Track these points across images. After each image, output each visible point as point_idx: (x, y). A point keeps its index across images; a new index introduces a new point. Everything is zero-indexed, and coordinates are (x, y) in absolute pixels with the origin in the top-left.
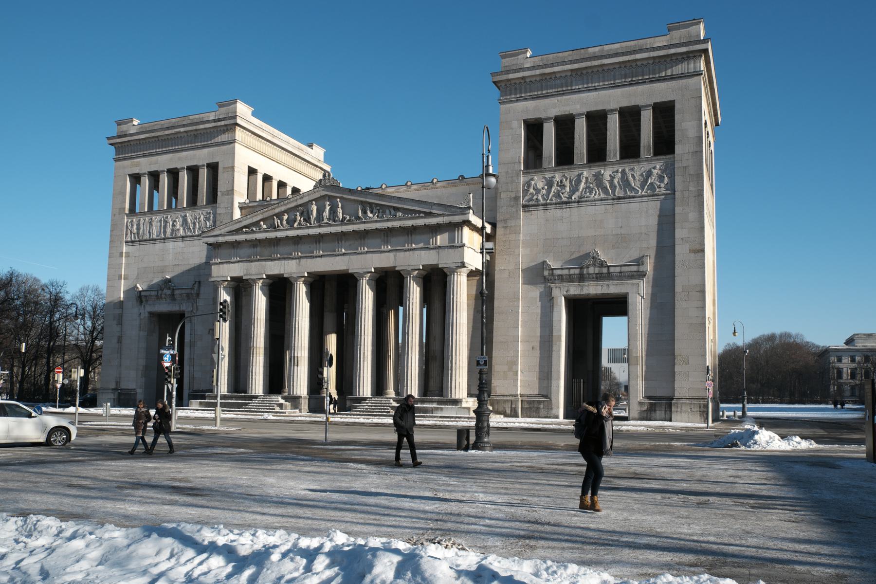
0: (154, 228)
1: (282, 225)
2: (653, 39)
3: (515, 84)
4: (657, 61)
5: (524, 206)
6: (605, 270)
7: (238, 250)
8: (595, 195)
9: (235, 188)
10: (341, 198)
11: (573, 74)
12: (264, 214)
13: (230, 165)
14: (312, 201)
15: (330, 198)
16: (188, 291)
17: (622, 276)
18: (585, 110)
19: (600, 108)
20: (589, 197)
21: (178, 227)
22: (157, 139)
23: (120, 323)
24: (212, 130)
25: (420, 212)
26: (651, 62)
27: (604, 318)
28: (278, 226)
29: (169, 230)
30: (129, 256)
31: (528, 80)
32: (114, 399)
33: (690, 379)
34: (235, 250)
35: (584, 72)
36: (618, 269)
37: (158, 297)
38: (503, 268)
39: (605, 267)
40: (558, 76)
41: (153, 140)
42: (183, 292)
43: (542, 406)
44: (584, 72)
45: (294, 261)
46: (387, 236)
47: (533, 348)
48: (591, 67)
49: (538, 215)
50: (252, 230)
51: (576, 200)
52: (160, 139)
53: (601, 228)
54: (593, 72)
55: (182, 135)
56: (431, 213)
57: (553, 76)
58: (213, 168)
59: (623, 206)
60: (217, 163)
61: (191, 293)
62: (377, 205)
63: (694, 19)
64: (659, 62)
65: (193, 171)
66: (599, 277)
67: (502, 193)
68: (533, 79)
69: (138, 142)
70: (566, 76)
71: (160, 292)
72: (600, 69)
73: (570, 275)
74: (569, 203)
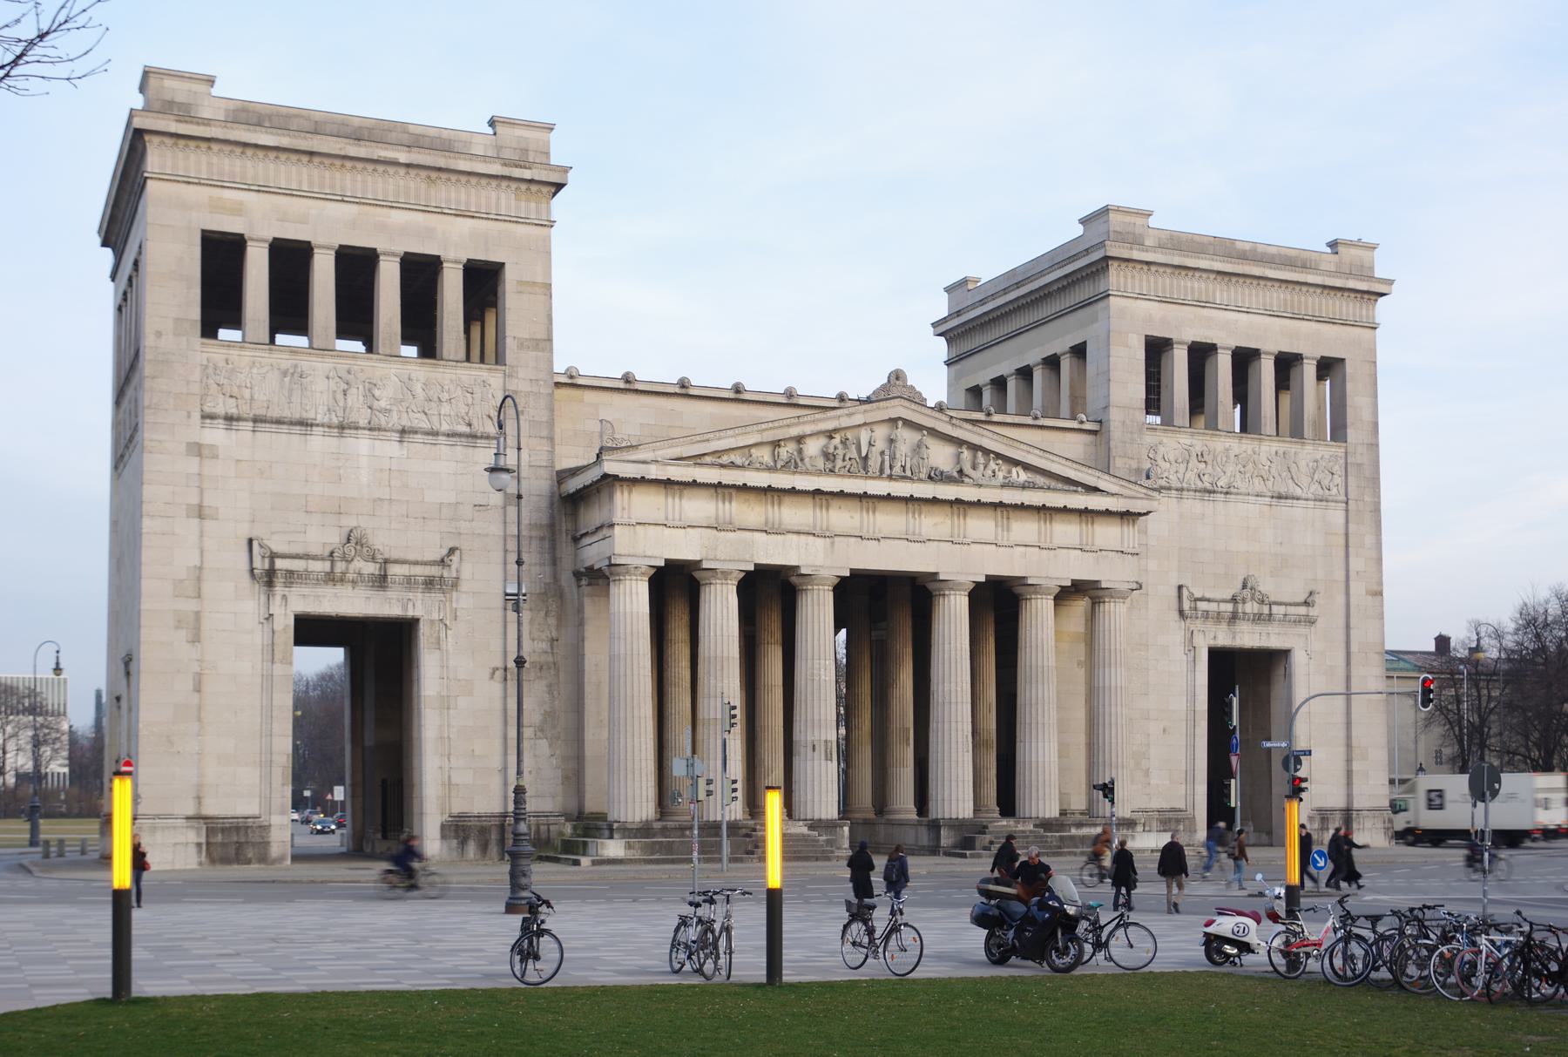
6: (1266, 610)
12: (765, 434)
13: (539, 279)
16: (434, 571)
18: (1234, 343)
19: (1253, 345)
21: (383, 404)
23: (196, 639)
32: (199, 845)
33: (1370, 782)
37: (331, 578)
42: (418, 570)
43: (1181, 827)
45: (820, 541)
47: (1164, 730)
51: (1225, 490)
56: (1096, 490)
59: (1284, 508)
61: (442, 577)
62: (999, 456)
66: (1258, 618)
67: (1117, 459)
71: (340, 567)
74: (1214, 492)
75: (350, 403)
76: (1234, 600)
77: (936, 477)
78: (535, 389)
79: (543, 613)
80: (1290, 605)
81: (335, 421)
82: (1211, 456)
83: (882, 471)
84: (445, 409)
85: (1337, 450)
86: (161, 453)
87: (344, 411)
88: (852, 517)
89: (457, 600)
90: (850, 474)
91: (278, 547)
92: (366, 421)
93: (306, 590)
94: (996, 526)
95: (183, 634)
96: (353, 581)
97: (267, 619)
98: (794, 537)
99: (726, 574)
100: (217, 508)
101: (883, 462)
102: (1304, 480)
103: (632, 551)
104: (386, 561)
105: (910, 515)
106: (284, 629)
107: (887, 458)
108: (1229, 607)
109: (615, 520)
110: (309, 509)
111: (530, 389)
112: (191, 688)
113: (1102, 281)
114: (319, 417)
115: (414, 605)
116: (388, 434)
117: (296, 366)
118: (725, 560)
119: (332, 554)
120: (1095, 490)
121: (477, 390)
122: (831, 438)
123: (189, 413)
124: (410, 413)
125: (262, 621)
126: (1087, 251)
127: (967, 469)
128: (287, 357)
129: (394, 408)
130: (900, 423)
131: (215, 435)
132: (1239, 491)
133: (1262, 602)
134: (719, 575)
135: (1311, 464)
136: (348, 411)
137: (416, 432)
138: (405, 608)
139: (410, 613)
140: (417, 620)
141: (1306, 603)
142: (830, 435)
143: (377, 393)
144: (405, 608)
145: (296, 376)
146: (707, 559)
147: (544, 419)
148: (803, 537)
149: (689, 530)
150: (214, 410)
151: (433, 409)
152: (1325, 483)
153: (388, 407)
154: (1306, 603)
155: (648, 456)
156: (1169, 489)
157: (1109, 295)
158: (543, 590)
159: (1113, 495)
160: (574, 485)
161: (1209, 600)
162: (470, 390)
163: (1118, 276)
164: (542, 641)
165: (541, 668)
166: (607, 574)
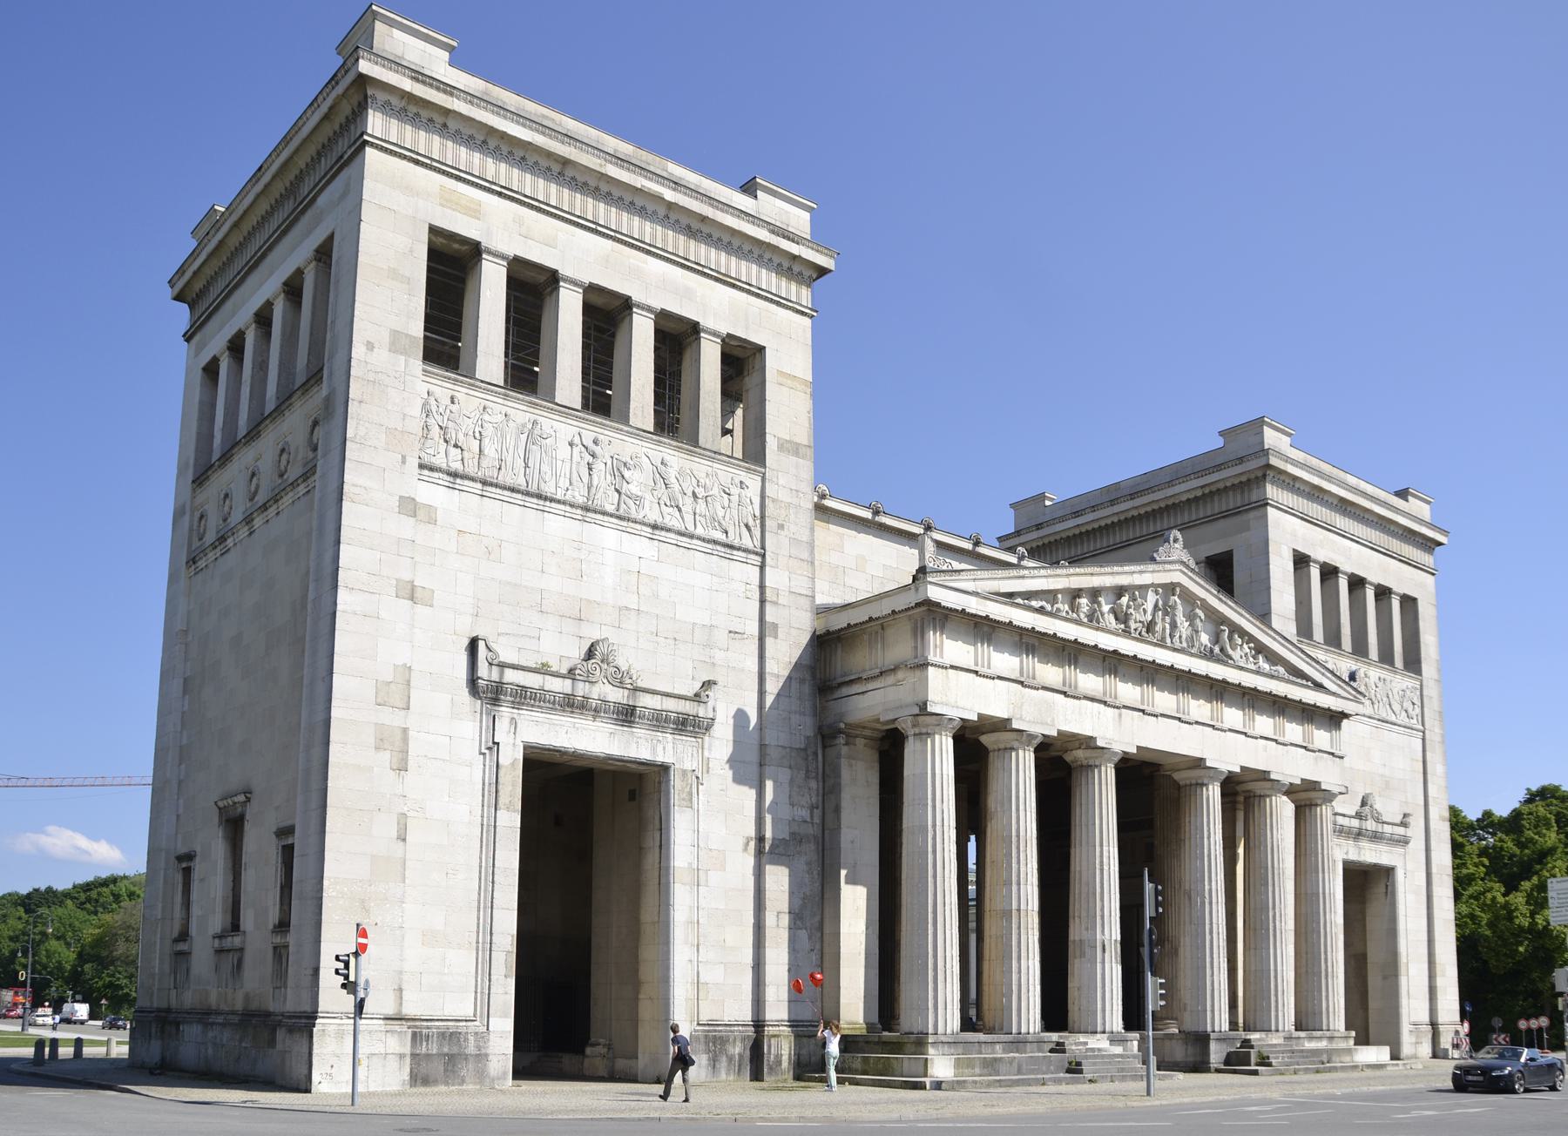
21: (634, 489)
23: (402, 767)
37: (570, 704)
42: (671, 705)
66: (1376, 837)
75: (595, 483)
77: (1208, 655)
78: (795, 501)
79: (802, 773)
81: (581, 500)
83: (1163, 639)
84: (701, 507)
85: (1401, 682)
87: (589, 489)
89: (710, 750)
90: (1140, 639)
91: (506, 656)
92: (613, 507)
93: (537, 715)
95: (385, 757)
96: (595, 710)
97: (490, 749)
98: (1089, 703)
99: (1031, 736)
100: (433, 591)
101: (1164, 629)
102: (1396, 707)
104: (636, 689)
106: (513, 764)
107: (1168, 626)
108: (1355, 823)
109: (931, 658)
110: (544, 608)
111: (789, 500)
112: (395, 834)
113: (1255, 491)
114: (559, 494)
115: (664, 748)
116: (638, 526)
117: (535, 423)
119: (571, 671)
120: (1319, 686)
121: (735, 491)
122: (1120, 596)
124: (663, 506)
125: (484, 751)
126: (1241, 460)
127: (1230, 652)
128: (525, 408)
129: (647, 497)
130: (1178, 590)
133: (1378, 820)
134: (1024, 738)
136: (593, 490)
137: (669, 530)
138: (654, 749)
139: (660, 758)
140: (664, 769)
142: (1119, 591)
143: (627, 474)
144: (654, 749)
145: (533, 436)
147: (805, 539)
148: (1096, 704)
150: (433, 460)
151: (687, 504)
152: (1410, 710)
153: (639, 494)
154: (1404, 824)
155: (969, 586)
157: (1267, 504)
158: (803, 746)
159: (1334, 694)
160: (839, 622)
161: (1344, 815)
162: (727, 490)
164: (803, 806)
165: (801, 842)
166: (905, 726)
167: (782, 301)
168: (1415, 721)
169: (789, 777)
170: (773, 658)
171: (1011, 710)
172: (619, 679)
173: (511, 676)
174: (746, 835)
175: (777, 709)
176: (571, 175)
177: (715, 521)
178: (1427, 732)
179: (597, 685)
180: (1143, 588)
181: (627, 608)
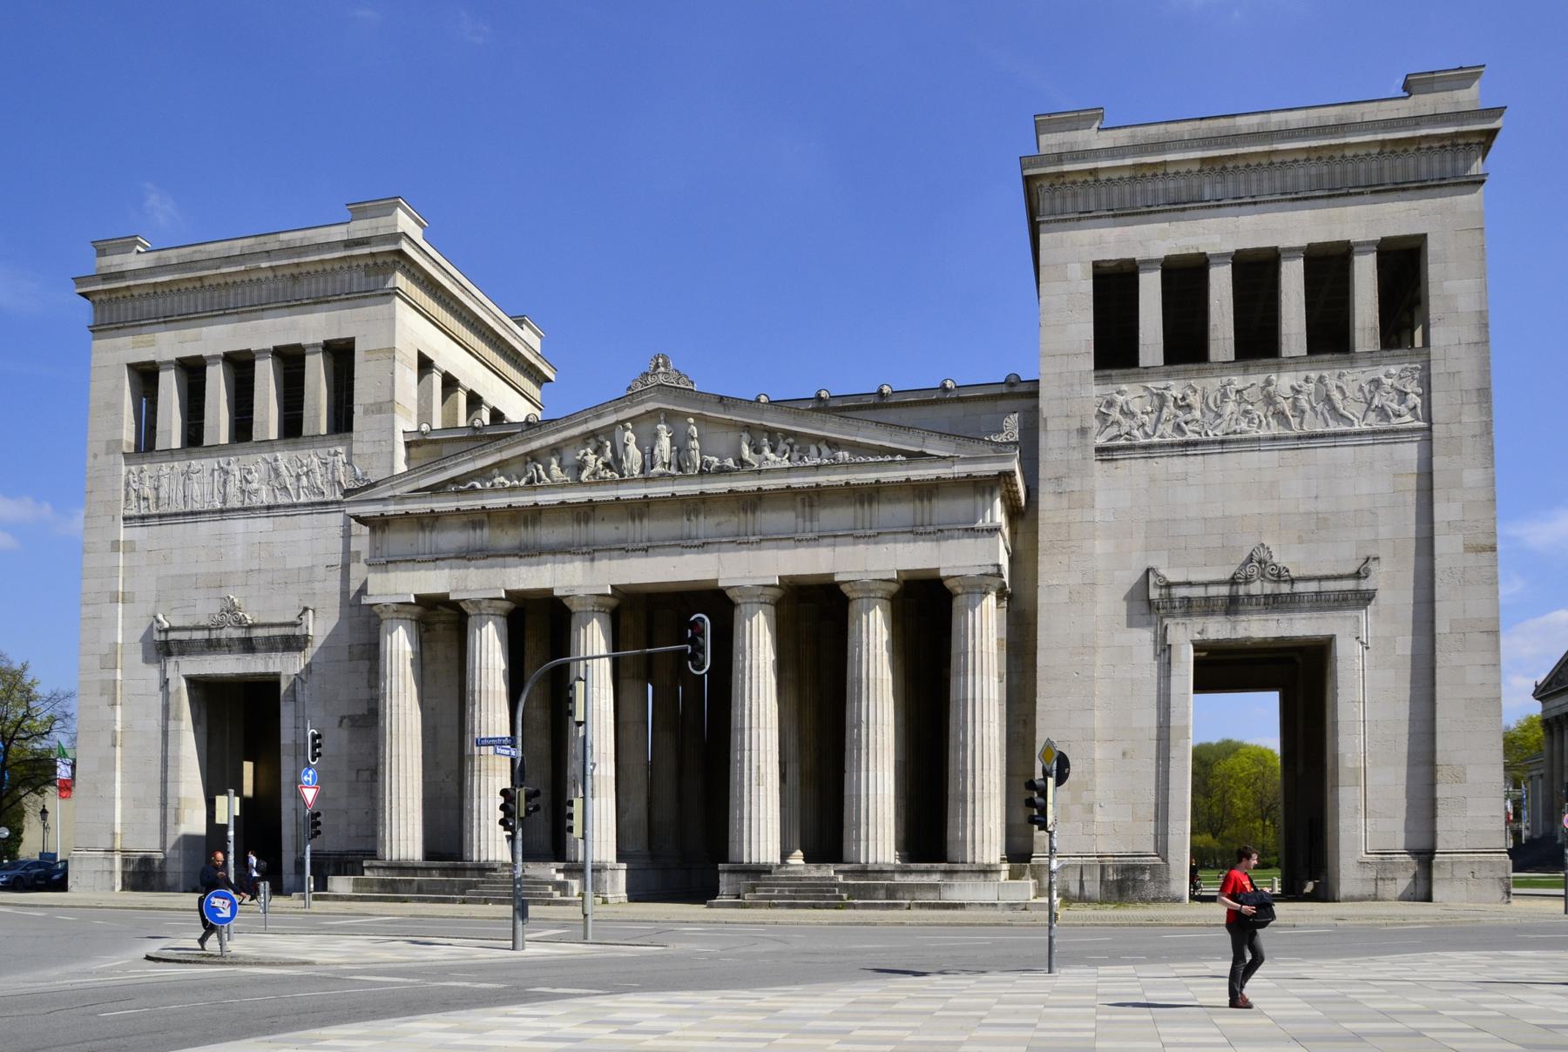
0: (196, 485)
1: (548, 475)
2: (1376, 104)
3: (1074, 183)
4: (1388, 149)
5: (1099, 450)
6: (1285, 588)
7: (434, 534)
8: (1260, 426)
9: (397, 398)
10: (700, 419)
11: (1204, 168)
14: (623, 422)
15: (670, 417)
17: (1323, 602)
20: (1246, 432)
22: (198, 285)
24: (337, 266)
25: (883, 451)
26: (1375, 151)
27: (1277, 693)
28: (539, 479)
29: (233, 489)
30: (133, 550)
31: (1103, 177)
34: (427, 534)
35: (1230, 165)
36: (1313, 587)
37: (212, 646)
38: (1054, 582)
39: (1285, 581)
40: (1171, 170)
41: (190, 286)
44: (1230, 165)
46: (811, 506)
47: (1124, 754)
48: (1244, 155)
49: (1133, 469)
50: (473, 487)
51: (1219, 438)
52: (206, 283)
53: (1272, 499)
54: (1248, 166)
55: (262, 276)
57: (1160, 172)
58: (341, 355)
59: (1322, 455)
60: (350, 343)
63: (1461, 68)
64: (1393, 152)
65: (290, 361)
66: (1274, 603)
68: (1115, 176)
69: (151, 291)
70: (1189, 172)
72: (1264, 161)
73: (1207, 599)
76: (1233, 582)
77: (704, 472)
80: (1327, 578)
82: (1198, 397)
86: (95, 552)
88: (617, 528)
94: (797, 517)
100: (134, 593)
102: (1353, 409)
103: (384, 591)
105: (685, 518)
118: (475, 590)
123: (113, 516)
131: (138, 533)
132: (1243, 436)
135: (1366, 388)
139: (271, 670)
141: (1357, 576)
146: (456, 590)
149: (438, 562)
156: (1132, 448)
161: (1189, 584)
163: (1052, 199)
167: (367, 294)
168: (1408, 418)
169: (368, 667)
170: (356, 579)
171: (454, 584)
172: (240, 623)
173: (173, 636)
174: (341, 714)
175: (360, 616)
176: (184, 287)
177: (313, 489)
178: (1434, 427)
179: (226, 628)
180: (609, 431)
181: (252, 571)
